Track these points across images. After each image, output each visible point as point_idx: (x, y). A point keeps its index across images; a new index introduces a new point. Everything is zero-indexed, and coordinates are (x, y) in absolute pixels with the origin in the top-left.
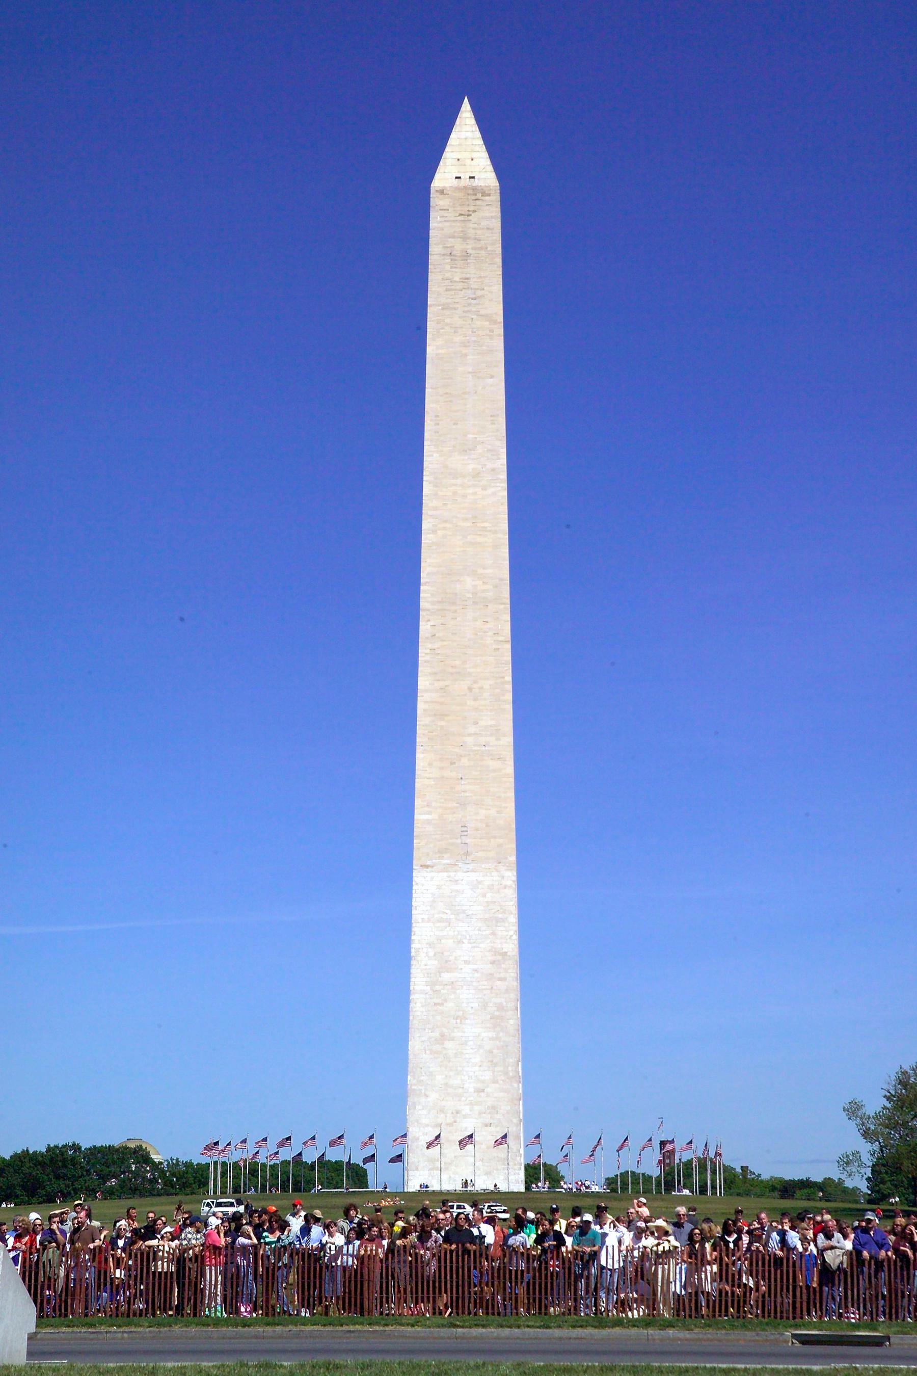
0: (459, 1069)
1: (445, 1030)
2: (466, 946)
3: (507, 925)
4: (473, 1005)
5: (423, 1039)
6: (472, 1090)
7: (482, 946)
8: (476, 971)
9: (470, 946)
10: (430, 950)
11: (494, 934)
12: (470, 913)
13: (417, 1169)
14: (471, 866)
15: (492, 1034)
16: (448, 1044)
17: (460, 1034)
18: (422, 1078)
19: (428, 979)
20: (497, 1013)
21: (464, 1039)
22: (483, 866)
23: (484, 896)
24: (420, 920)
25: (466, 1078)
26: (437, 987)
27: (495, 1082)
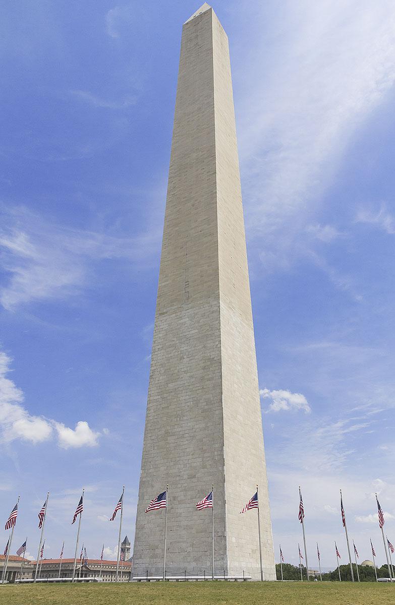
0: (178, 459)
1: (168, 428)
2: (186, 360)
3: (213, 338)
4: (189, 404)
5: (153, 438)
6: (186, 477)
7: (196, 357)
8: (191, 377)
9: (188, 359)
10: (161, 369)
11: (205, 347)
12: (189, 336)
13: (141, 558)
14: (190, 306)
15: (204, 425)
16: (171, 439)
17: (180, 429)
18: (150, 471)
19: (160, 391)
20: (206, 407)
21: (181, 433)
22: (198, 303)
23: (199, 322)
24: (157, 350)
25: (182, 466)
26: (165, 395)
27: (204, 467)
